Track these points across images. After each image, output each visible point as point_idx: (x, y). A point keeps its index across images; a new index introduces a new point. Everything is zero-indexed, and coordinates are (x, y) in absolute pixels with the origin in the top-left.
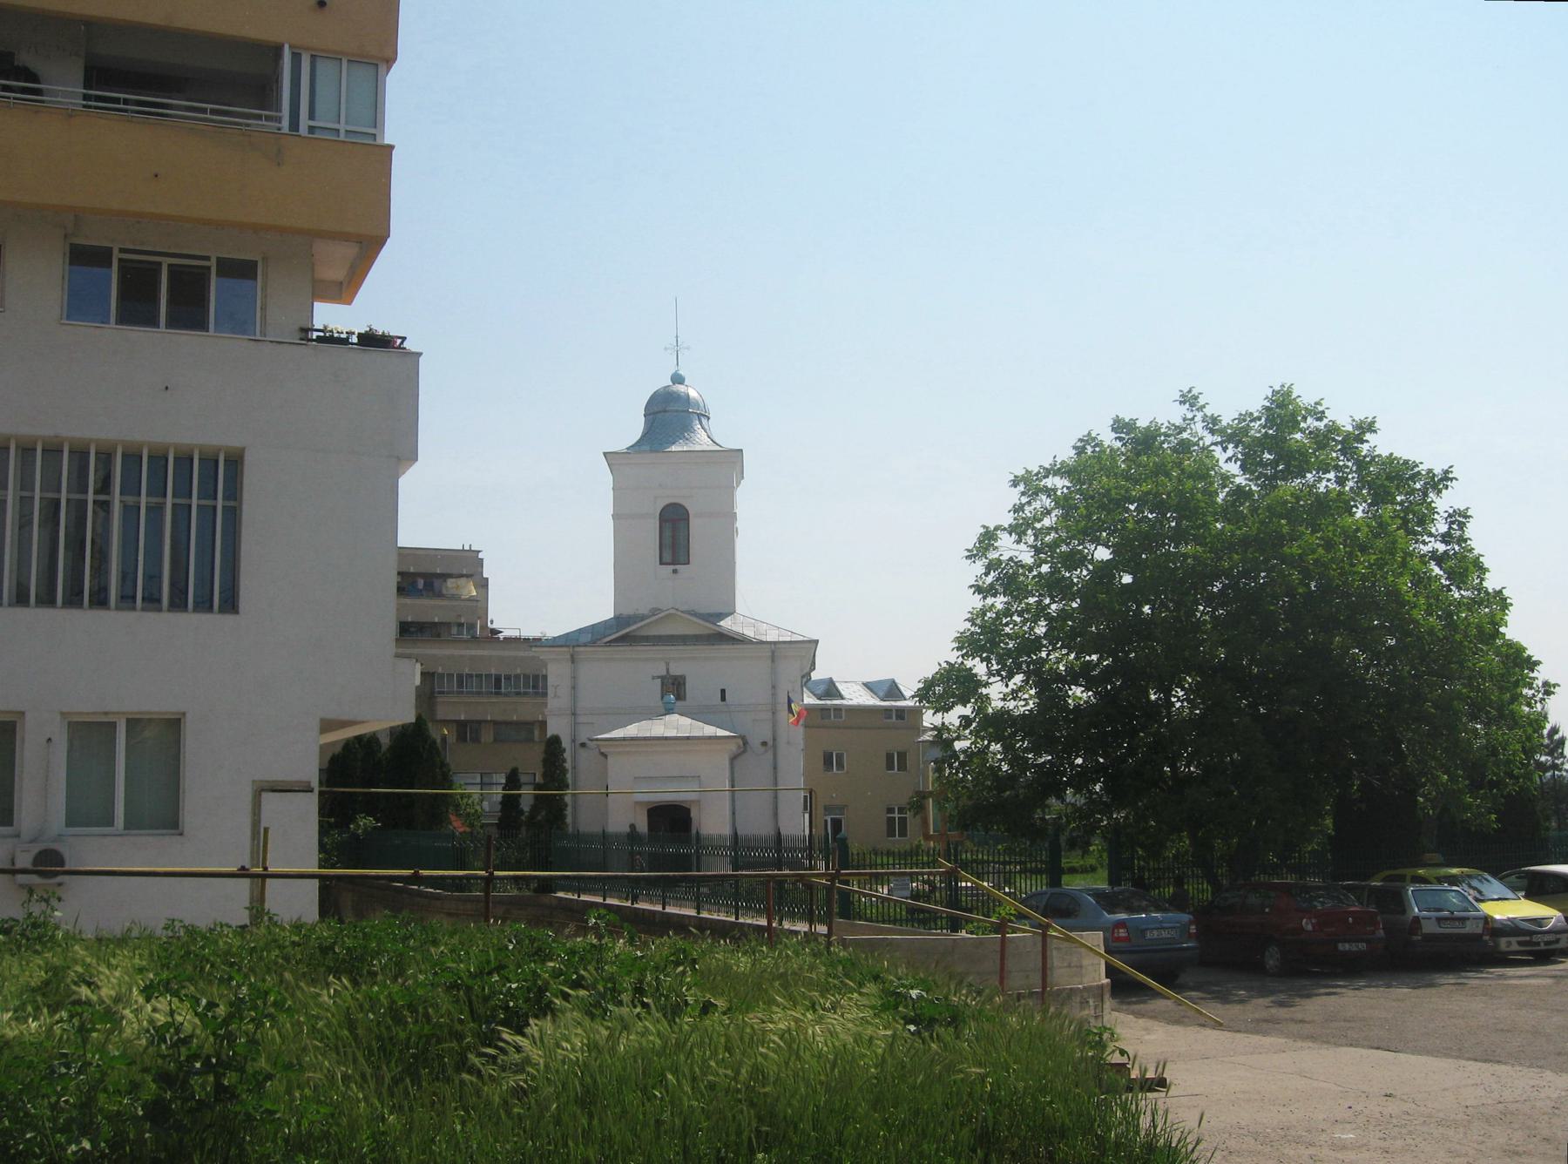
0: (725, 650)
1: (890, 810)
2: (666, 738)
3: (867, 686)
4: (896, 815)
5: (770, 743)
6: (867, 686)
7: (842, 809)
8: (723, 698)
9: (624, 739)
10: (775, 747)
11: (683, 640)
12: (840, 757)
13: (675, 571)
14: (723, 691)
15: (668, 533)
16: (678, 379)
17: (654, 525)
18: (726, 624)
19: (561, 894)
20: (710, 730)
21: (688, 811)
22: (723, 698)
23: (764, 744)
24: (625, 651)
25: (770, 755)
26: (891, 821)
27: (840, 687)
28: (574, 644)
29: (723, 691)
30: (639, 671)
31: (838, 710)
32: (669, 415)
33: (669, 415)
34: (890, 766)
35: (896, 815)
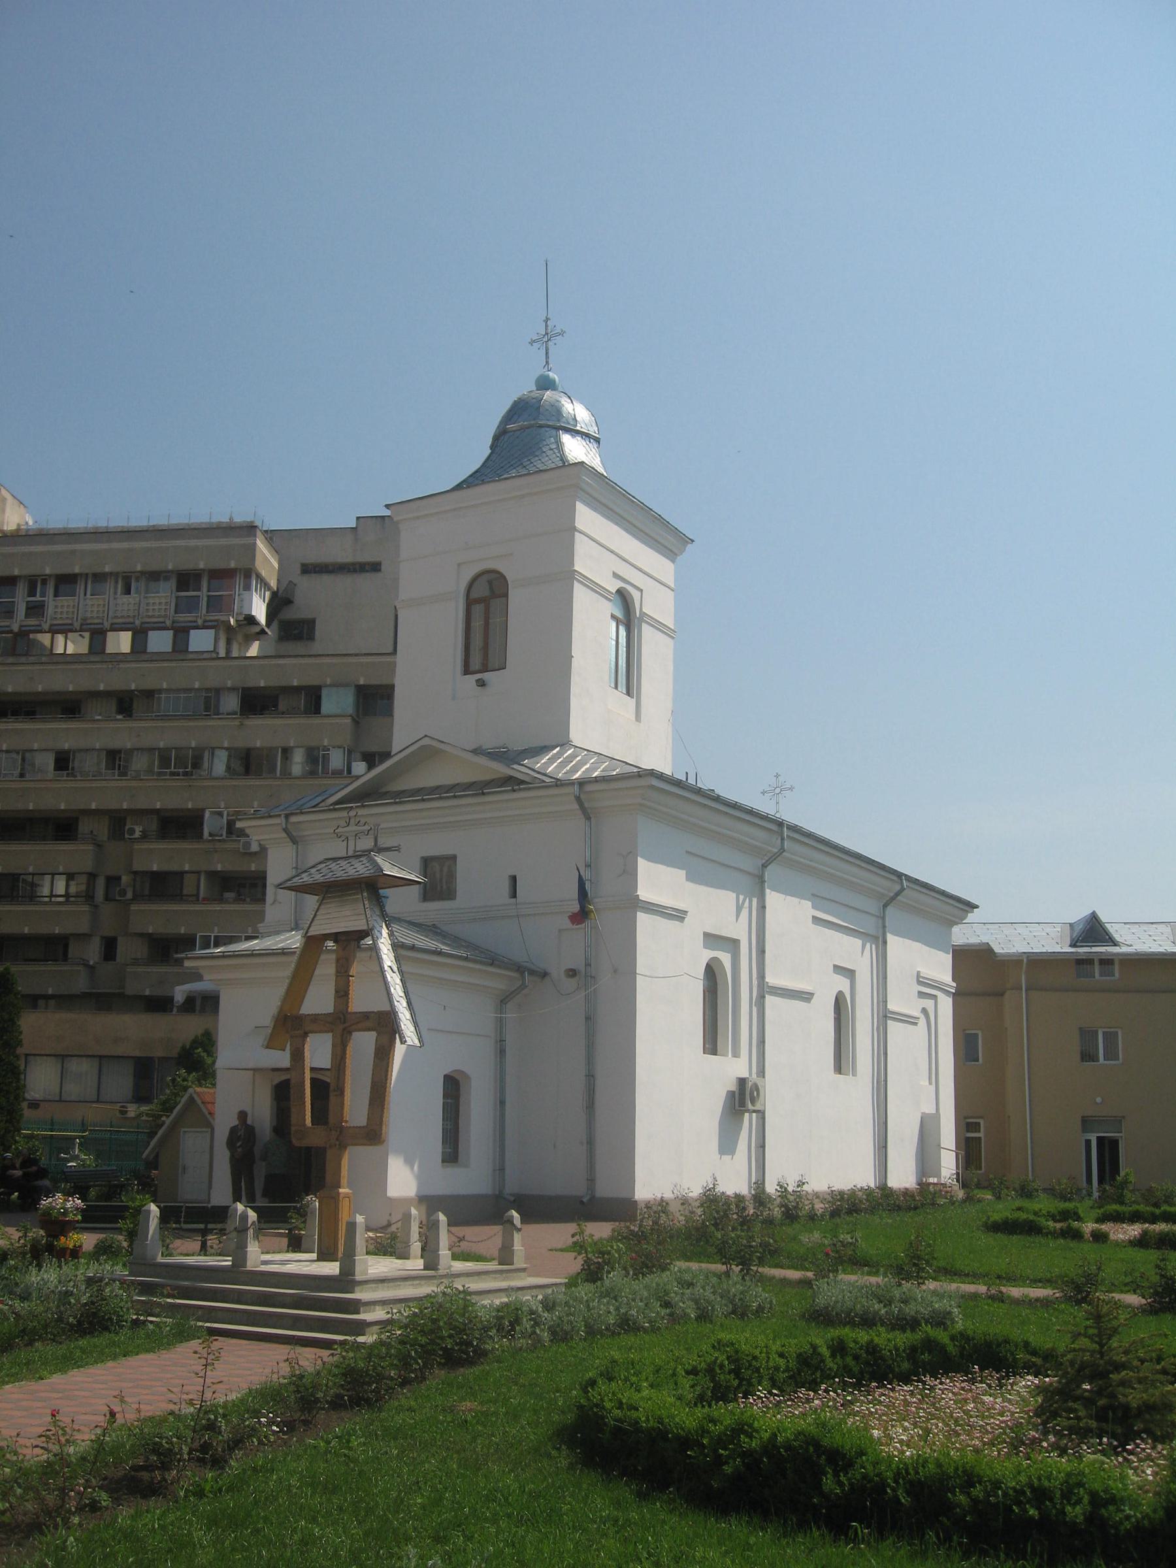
7: (1117, 1122)
12: (1111, 1038)
14: (514, 879)
15: (477, 624)
16: (545, 384)
22: (514, 895)
23: (572, 973)
27: (1111, 929)
31: (1107, 962)
32: (524, 436)
33: (524, 436)
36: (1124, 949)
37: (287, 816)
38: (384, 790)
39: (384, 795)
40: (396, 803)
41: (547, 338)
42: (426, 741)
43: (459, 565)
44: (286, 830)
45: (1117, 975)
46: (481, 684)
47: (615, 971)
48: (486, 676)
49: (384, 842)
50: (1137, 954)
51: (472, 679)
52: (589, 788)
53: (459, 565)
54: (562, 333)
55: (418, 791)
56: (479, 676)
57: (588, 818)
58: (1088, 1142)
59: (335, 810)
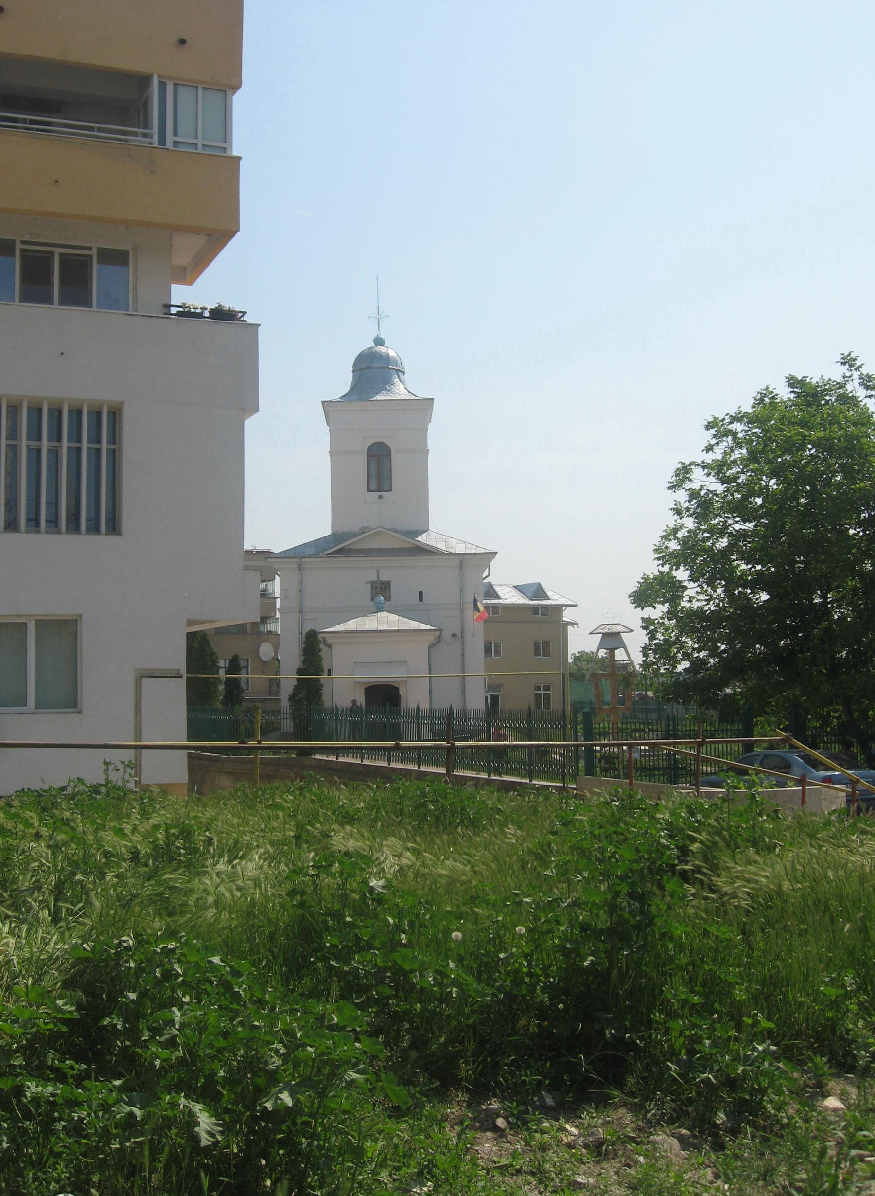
0: (422, 561)
1: (539, 688)
2: (380, 631)
3: (518, 588)
4: (542, 692)
5: (459, 635)
6: (518, 588)
7: (499, 687)
8: (421, 599)
9: (346, 632)
10: (462, 637)
12: (497, 646)
13: (380, 497)
14: (421, 593)
15: (374, 466)
16: (379, 341)
17: (363, 459)
18: (422, 539)
19: (318, 757)
20: (414, 625)
21: (397, 689)
22: (421, 599)
23: (454, 635)
24: (342, 560)
25: (459, 643)
26: (538, 696)
28: (300, 557)
29: (421, 593)
30: (357, 576)
32: (373, 370)
33: (373, 370)
34: (537, 653)
35: (542, 692)
36: (506, 602)
41: (378, 318)
42: (380, 529)
50: (513, 604)
54: (387, 316)
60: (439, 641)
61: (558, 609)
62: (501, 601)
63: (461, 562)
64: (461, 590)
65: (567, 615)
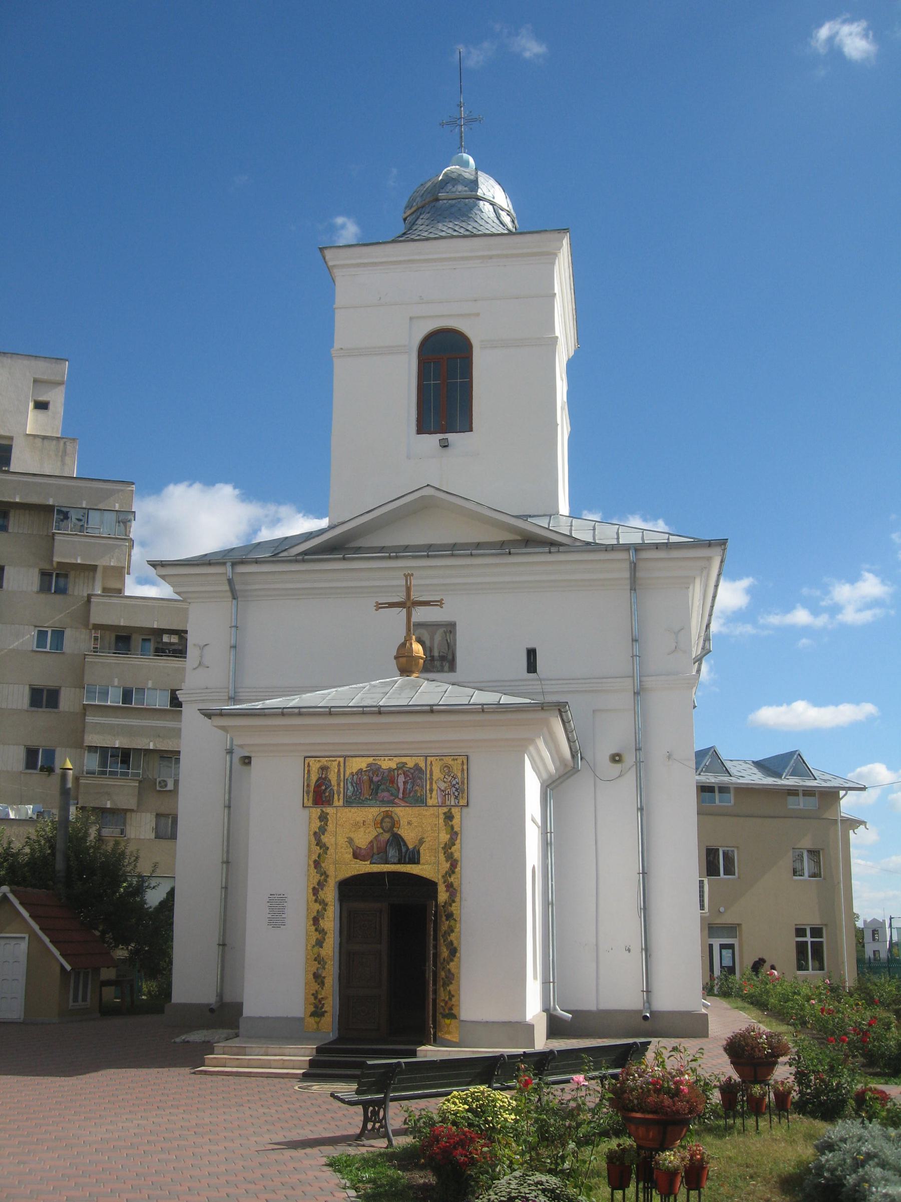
1: (800, 932)
2: (380, 711)
3: (759, 765)
4: (808, 939)
6: (759, 765)
8: (532, 667)
11: (453, 549)
13: (445, 445)
14: (532, 654)
22: (532, 667)
25: (630, 778)
26: (801, 948)
27: (728, 765)
29: (532, 654)
31: (724, 789)
35: (808, 939)
36: (741, 781)
37: (234, 564)
38: (353, 545)
39: (358, 550)
40: (390, 558)
43: (411, 318)
44: (230, 582)
45: (732, 802)
46: (445, 445)
47: (669, 757)
48: (450, 436)
49: (414, 596)
51: (434, 440)
52: (644, 555)
53: (411, 318)
55: (406, 548)
56: (441, 436)
57: (633, 588)
58: (711, 946)
59: (304, 561)
60: (575, 770)
61: (830, 796)
62: (734, 780)
63: (634, 568)
64: (635, 640)
65: (848, 804)
